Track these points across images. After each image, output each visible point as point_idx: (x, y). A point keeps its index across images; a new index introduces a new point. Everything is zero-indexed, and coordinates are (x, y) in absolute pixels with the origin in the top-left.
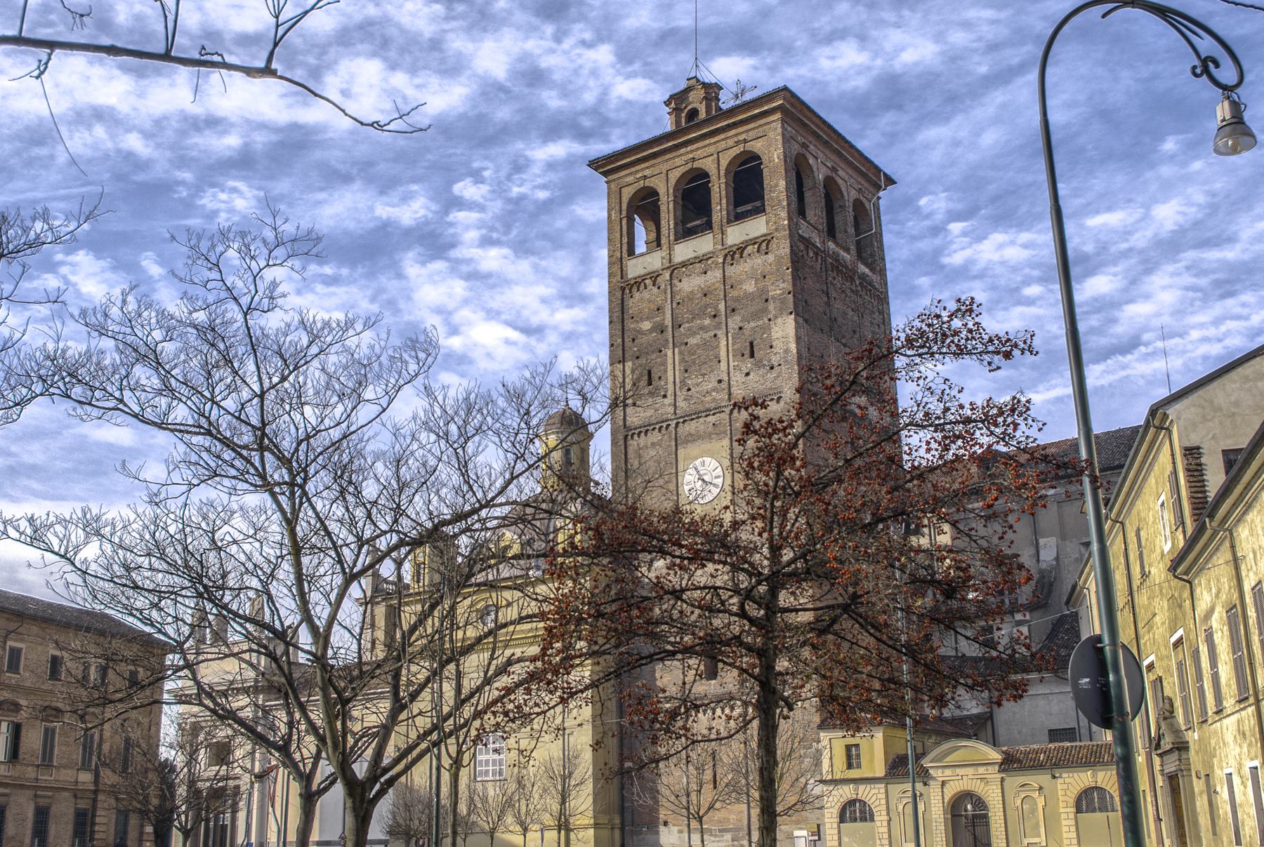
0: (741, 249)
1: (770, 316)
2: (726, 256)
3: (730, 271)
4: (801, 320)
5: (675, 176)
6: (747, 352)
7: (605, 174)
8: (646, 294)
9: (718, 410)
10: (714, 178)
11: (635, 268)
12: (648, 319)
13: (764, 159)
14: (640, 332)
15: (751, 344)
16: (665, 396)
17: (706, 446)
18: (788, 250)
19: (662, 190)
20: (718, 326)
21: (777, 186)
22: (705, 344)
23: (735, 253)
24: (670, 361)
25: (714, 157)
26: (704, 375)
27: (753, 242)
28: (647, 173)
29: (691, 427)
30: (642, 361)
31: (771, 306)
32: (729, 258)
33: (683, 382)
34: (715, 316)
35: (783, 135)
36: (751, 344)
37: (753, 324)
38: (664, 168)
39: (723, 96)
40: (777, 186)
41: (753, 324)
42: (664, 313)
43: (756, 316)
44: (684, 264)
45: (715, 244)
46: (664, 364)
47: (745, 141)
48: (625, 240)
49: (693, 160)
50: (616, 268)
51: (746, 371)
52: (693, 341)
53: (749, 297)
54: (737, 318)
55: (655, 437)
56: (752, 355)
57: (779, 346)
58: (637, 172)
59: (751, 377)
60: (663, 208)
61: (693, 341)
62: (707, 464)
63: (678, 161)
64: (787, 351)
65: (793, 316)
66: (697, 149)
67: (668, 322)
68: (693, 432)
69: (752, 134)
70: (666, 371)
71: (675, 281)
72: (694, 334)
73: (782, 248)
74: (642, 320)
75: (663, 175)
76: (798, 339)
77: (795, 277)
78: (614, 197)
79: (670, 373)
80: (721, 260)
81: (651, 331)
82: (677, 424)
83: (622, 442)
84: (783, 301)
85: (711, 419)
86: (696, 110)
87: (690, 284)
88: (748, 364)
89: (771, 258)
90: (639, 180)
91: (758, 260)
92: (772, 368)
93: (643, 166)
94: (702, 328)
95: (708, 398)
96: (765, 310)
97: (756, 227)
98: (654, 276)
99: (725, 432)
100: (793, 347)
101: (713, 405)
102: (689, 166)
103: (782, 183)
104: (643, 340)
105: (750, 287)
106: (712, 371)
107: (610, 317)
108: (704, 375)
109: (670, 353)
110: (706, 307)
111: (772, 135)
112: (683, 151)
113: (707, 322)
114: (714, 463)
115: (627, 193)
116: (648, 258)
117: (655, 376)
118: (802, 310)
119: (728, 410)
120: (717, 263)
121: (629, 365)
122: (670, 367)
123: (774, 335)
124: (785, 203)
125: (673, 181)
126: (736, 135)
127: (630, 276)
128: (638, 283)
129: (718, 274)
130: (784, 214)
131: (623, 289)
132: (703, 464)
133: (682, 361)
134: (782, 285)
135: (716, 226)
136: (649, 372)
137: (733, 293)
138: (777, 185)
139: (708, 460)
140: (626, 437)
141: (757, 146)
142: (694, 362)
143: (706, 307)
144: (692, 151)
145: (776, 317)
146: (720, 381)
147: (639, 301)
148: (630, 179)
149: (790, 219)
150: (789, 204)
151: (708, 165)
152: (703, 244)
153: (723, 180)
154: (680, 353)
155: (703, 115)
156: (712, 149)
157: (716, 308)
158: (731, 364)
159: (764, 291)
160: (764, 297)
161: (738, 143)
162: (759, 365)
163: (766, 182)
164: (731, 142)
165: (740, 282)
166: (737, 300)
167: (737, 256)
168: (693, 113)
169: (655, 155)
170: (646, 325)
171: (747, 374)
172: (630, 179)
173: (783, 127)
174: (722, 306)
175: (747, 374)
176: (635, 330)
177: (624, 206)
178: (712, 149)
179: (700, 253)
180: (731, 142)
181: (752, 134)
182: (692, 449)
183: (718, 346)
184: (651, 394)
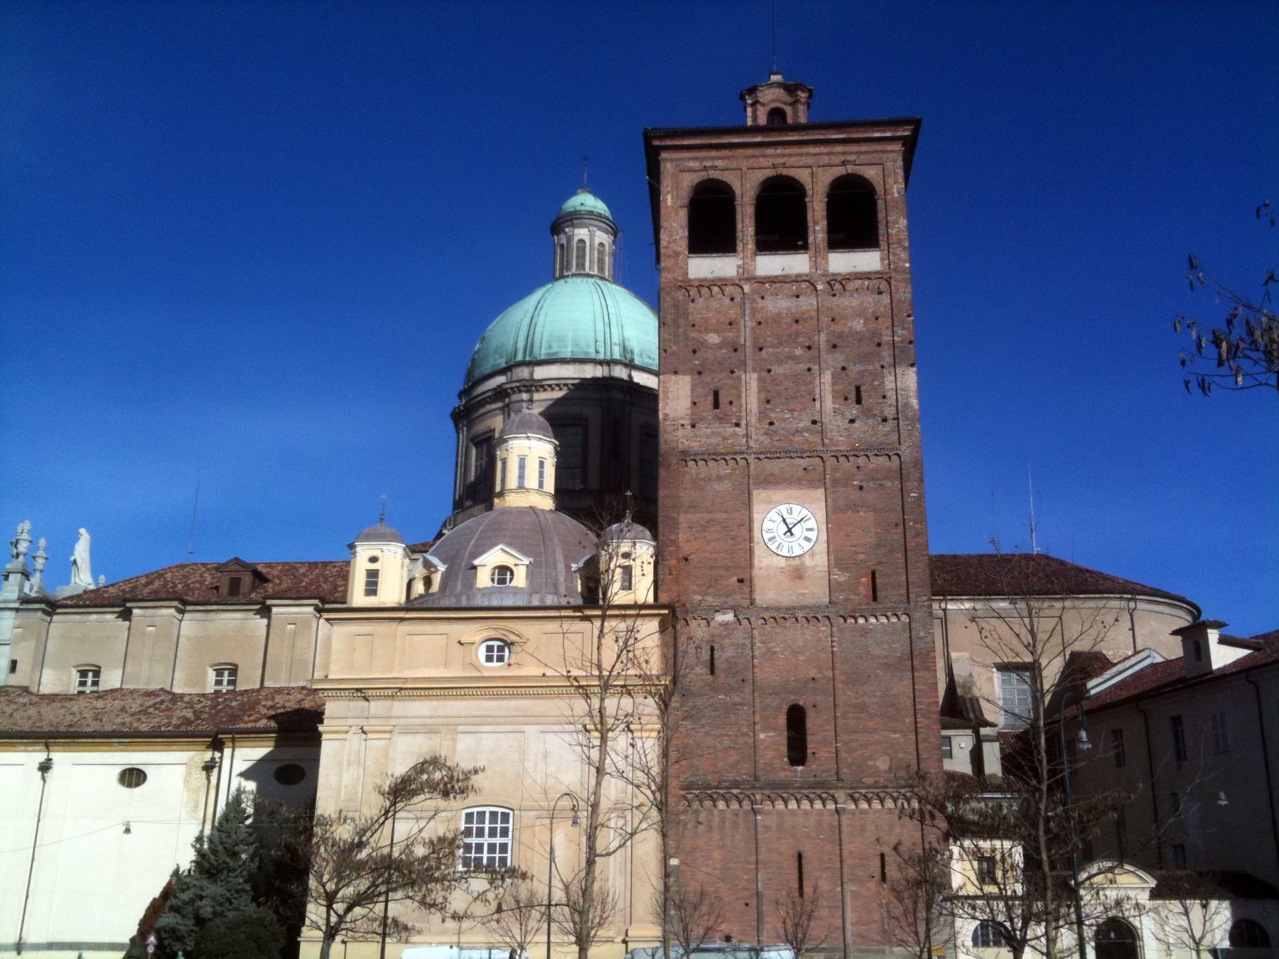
6: (853, 396)
15: (858, 389)
16: (737, 425)
22: (795, 377)
23: (839, 283)
29: (773, 466)
34: (809, 348)
36: (858, 389)
37: (859, 367)
52: (778, 370)
56: (859, 401)
59: (856, 425)
61: (778, 370)
65: (915, 369)
72: (780, 362)
85: (803, 463)
87: (778, 304)
88: (854, 411)
92: (885, 420)
94: (792, 357)
97: (867, 260)
105: (858, 325)
106: (804, 409)
108: (792, 411)
110: (798, 334)
113: (799, 352)
126: (844, 153)
135: (811, 246)
142: (779, 394)
143: (798, 334)
156: (810, 161)
160: (876, 340)
161: (844, 163)
162: (868, 413)
164: (836, 160)
166: (840, 335)
171: (852, 421)
175: (852, 421)
178: (810, 161)
180: (836, 160)
182: (777, 494)
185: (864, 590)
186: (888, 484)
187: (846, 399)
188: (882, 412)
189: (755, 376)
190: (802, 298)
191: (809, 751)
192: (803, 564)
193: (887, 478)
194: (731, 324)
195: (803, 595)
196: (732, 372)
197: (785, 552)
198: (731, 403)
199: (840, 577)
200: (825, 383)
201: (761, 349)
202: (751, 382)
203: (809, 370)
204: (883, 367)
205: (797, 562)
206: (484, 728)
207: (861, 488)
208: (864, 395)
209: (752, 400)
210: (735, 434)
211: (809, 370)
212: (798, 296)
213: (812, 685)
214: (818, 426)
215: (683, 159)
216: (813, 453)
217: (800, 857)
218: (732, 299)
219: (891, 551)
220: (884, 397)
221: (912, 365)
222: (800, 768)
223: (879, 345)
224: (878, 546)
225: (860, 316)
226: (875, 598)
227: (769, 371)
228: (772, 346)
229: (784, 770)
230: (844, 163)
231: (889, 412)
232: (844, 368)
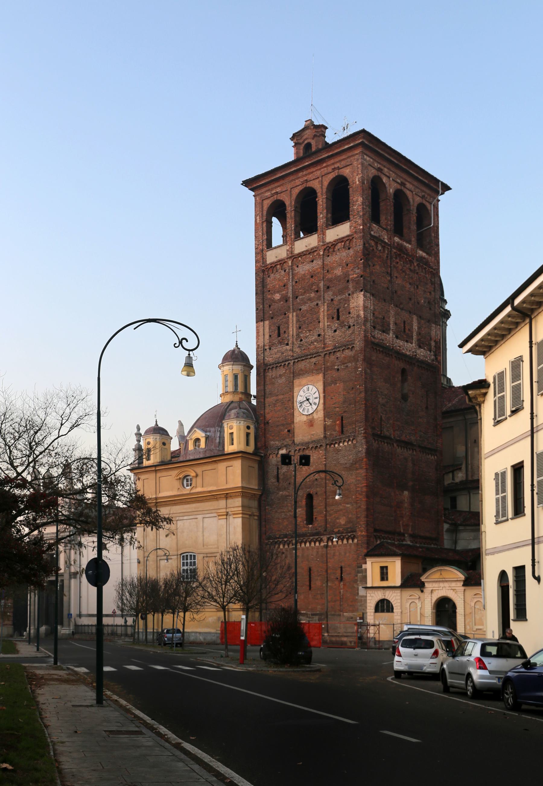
0: (334, 244)
1: (350, 292)
2: (325, 250)
3: (328, 260)
4: (368, 295)
5: (296, 191)
6: (335, 316)
7: (252, 190)
8: (277, 276)
9: (317, 354)
10: (319, 195)
11: (271, 257)
12: (278, 292)
13: (350, 181)
14: (274, 301)
15: (338, 310)
16: (287, 344)
17: (310, 378)
18: (361, 247)
19: (287, 203)
20: (319, 298)
21: (358, 202)
23: (330, 248)
24: (291, 321)
25: (320, 181)
26: (310, 331)
27: (341, 240)
28: (278, 190)
29: (302, 365)
30: (275, 320)
31: (351, 286)
32: (326, 251)
33: (298, 335)
34: (317, 291)
35: (362, 164)
36: (338, 310)
37: (339, 297)
38: (289, 186)
39: (328, 133)
40: (358, 202)
41: (339, 297)
42: (287, 288)
43: (341, 292)
44: (301, 255)
45: (319, 241)
46: (287, 323)
47: (339, 168)
48: (265, 237)
49: (307, 181)
50: (259, 257)
51: (334, 329)
52: (304, 308)
53: (338, 278)
54: (330, 293)
55: (282, 371)
56: (338, 319)
57: (354, 313)
58: (272, 189)
60: (288, 215)
61: (304, 308)
62: (310, 389)
63: (298, 182)
64: (358, 316)
65: (362, 293)
66: (309, 174)
67: (290, 295)
68: (303, 368)
69: (343, 163)
70: (288, 328)
71: (295, 267)
72: (305, 303)
73: (358, 245)
74: (275, 293)
75: (288, 192)
76: (365, 308)
77: (366, 265)
78: (259, 205)
79: (291, 329)
80: (321, 253)
81: (280, 300)
82: (294, 362)
83: (262, 374)
84: (357, 282)
85: (313, 360)
86: (310, 142)
87: (304, 269)
89: (351, 252)
90: (273, 195)
91: (344, 254)
92: (349, 327)
93: (276, 185)
94: (310, 299)
95: (312, 347)
96: (347, 288)
97: (343, 230)
98: (282, 262)
99: (321, 369)
100: (362, 313)
101: (315, 351)
102: (304, 185)
103: (360, 199)
104: (275, 306)
105: (338, 272)
107: (256, 290)
108: (310, 331)
109: (291, 316)
110: (313, 284)
111: (355, 163)
112: (301, 174)
113: (313, 295)
114: (315, 390)
115: (267, 203)
116: (278, 250)
117: (282, 331)
118: (369, 287)
119: (323, 355)
120: (320, 255)
121: (267, 322)
122: (291, 325)
123: (352, 305)
124: (361, 214)
125: (294, 196)
126: (333, 164)
127: (268, 262)
128: (273, 267)
129: (320, 262)
130: (360, 221)
131: (263, 271)
132: (308, 389)
133: (298, 321)
134: (357, 271)
136: (279, 328)
137: (329, 276)
138: (357, 201)
139: (311, 387)
140: (265, 370)
141: (346, 172)
144: (306, 175)
145: (353, 293)
146: (319, 335)
147: (273, 280)
148: (268, 194)
149: (364, 224)
150: (364, 215)
151: (315, 185)
152: (310, 242)
153: (325, 197)
154: (297, 316)
155: (314, 149)
157: (318, 285)
158: (326, 324)
159: (346, 275)
160: (347, 279)
161: (334, 169)
162: (342, 325)
163: (351, 198)
164: (330, 169)
165: (333, 268)
166: (330, 280)
167: (331, 250)
168: (308, 146)
169: (283, 177)
170: (277, 296)
172: (268, 194)
173: (363, 158)
174: (321, 285)
175: (335, 331)
176: (270, 299)
177: (265, 213)
179: (310, 247)
180: (330, 169)
181: (343, 163)
182: (303, 380)
183: (318, 312)
184: (280, 343)
185: (338, 428)
186: (350, 365)
187: (333, 318)
188: (348, 322)
189: (295, 314)
190: (315, 262)
191: (314, 517)
192: (313, 418)
193: (349, 362)
194: (284, 286)
195: (313, 435)
196: (285, 314)
197: (306, 413)
198: (285, 332)
199: (328, 423)
200: (323, 310)
201: (297, 298)
202: (292, 317)
203: (317, 304)
204: (349, 295)
205: (310, 417)
206: (185, 518)
207: (338, 370)
208: (341, 314)
209: (292, 330)
210: (287, 350)
211: (317, 304)
212: (312, 261)
213: (316, 483)
214: (321, 338)
215: (262, 193)
216: (317, 354)
217: (310, 569)
218: (285, 271)
219: (350, 404)
220: (349, 313)
221: (362, 291)
222: (310, 526)
223: (348, 281)
224: (344, 402)
225: (340, 266)
226: (342, 432)
227: (300, 309)
228: (301, 295)
229: (304, 527)
230: (334, 169)
231: (351, 323)
232: (332, 300)
